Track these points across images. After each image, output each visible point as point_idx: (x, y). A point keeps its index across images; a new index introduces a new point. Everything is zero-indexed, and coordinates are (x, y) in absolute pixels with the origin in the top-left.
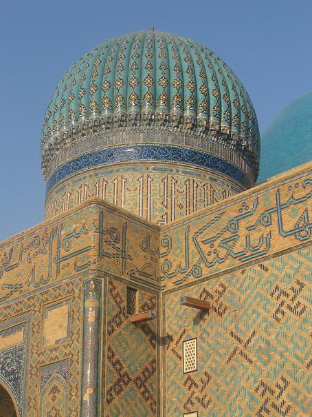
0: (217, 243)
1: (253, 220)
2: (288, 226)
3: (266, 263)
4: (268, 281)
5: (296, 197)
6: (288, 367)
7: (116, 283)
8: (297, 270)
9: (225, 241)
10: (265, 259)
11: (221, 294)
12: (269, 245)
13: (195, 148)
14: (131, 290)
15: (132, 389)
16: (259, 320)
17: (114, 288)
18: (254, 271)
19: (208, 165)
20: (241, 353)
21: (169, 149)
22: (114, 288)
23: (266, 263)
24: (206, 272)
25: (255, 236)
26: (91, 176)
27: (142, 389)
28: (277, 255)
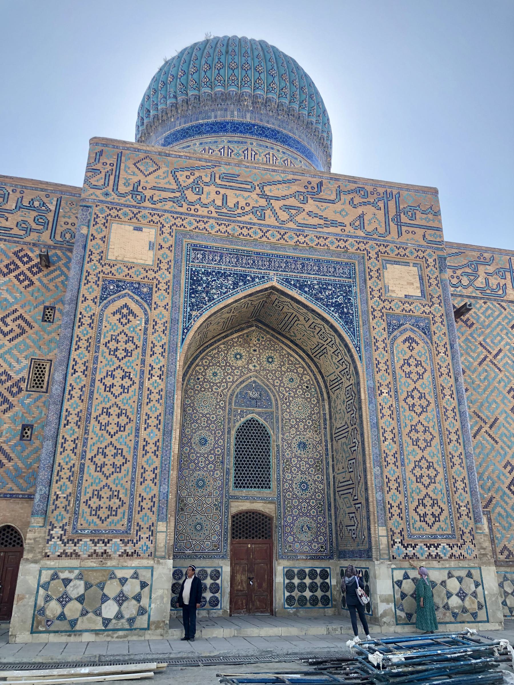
0: (459, 272)
1: (491, 269)
4: (506, 317)
10: (502, 301)
12: (505, 292)
16: (503, 343)
18: (495, 306)
20: (491, 361)
23: (503, 304)
25: (493, 281)
26: (278, 151)
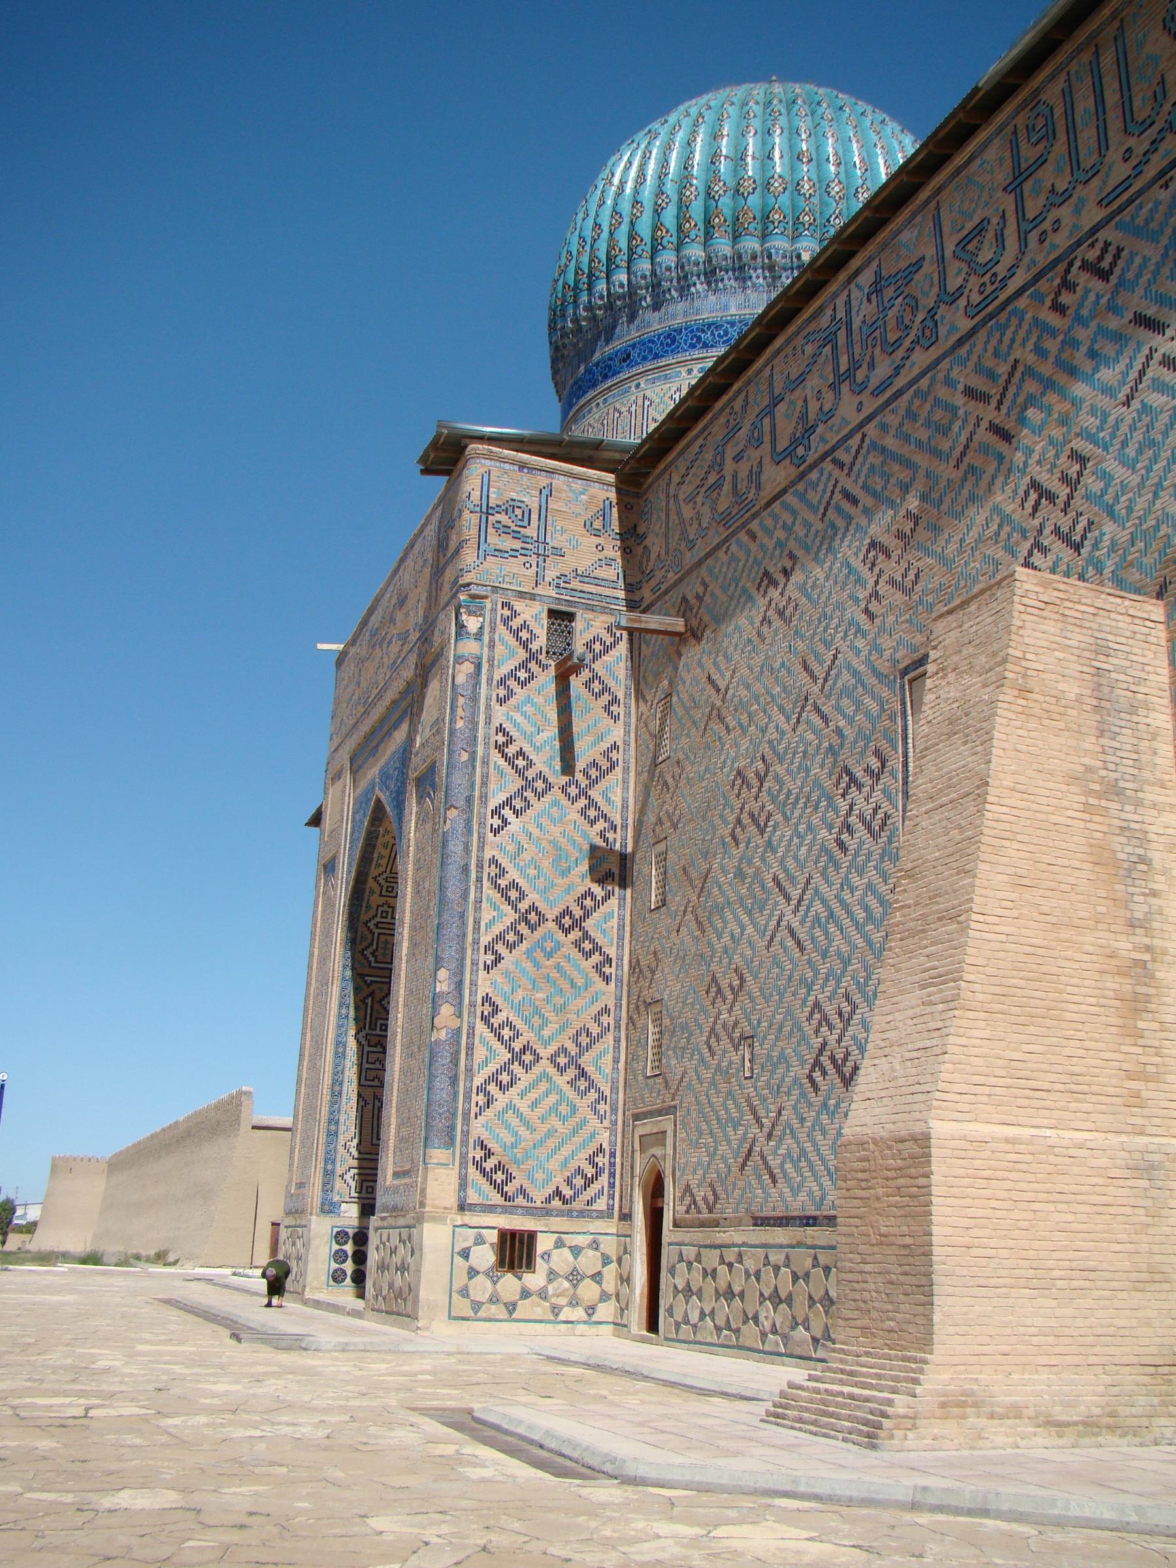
3: (754, 525)
7: (519, 606)
14: (561, 617)
15: (555, 803)
17: (515, 614)
21: (732, 324)
22: (515, 614)
24: (689, 559)
27: (583, 802)
28: (769, 504)
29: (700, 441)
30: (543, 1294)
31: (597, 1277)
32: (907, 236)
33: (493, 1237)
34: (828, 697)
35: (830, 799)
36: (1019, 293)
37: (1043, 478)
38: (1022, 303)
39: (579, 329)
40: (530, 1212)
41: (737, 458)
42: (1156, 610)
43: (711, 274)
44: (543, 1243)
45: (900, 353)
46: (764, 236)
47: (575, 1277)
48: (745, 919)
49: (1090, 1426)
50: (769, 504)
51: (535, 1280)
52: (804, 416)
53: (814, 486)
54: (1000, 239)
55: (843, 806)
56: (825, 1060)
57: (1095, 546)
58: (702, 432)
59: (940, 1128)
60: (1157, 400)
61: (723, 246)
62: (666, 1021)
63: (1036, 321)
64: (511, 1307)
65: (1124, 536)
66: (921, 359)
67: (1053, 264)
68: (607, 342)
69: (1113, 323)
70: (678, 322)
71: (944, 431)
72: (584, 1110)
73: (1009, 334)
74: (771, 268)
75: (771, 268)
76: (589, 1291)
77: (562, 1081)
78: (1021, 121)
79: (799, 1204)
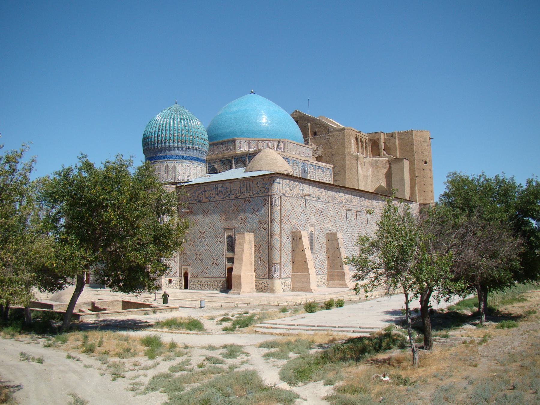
2: (207, 196)
3: (202, 204)
5: (209, 189)
6: (205, 228)
8: (208, 207)
9: (193, 196)
11: (192, 208)
12: (202, 199)
13: (188, 155)
19: (192, 160)
23: (202, 204)
25: (199, 197)
28: (204, 202)
29: (191, 188)
30: (173, 286)
31: (177, 284)
32: (226, 184)
33: (168, 280)
34: (214, 227)
35: (214, 238)
36: (240, 198)
37: (242, 217)
38: (241, 200)
39: (155, 149)
40: (171, 277)
41: (199, 194)
42: (253, 234)
43: (178, 148)
44: (172, 280)
45: (225, 196)
46: (185, 144)
47: (175, 284)
48: (201, 247)
49: (249, 293)
50: (204, 202)
51: (172, 284)
52: (210, 195)
53: (212, 204)
54: (238, 192)
55: (217, 239)
56: (214, 263)
57: (247, 226)
58: (192, 187)
59: (242, 274)
60: (254, 216)
61: (180, 144)
62: (187, 256)
63: (242, 203)
64: (170, 288)
65: (250, 226)
66: (227, 198)
67: (244, 198)
68: (161, 153)
69: (250, 207)
70: (173, 154)
71: (231, 207)
72: (175, 265)
73: (239, 202)
74: (186, 148)
75: (186, 148)
76: (176, 285)
77: (173, 262)
78: (241, 182)
79: (211, 276)
